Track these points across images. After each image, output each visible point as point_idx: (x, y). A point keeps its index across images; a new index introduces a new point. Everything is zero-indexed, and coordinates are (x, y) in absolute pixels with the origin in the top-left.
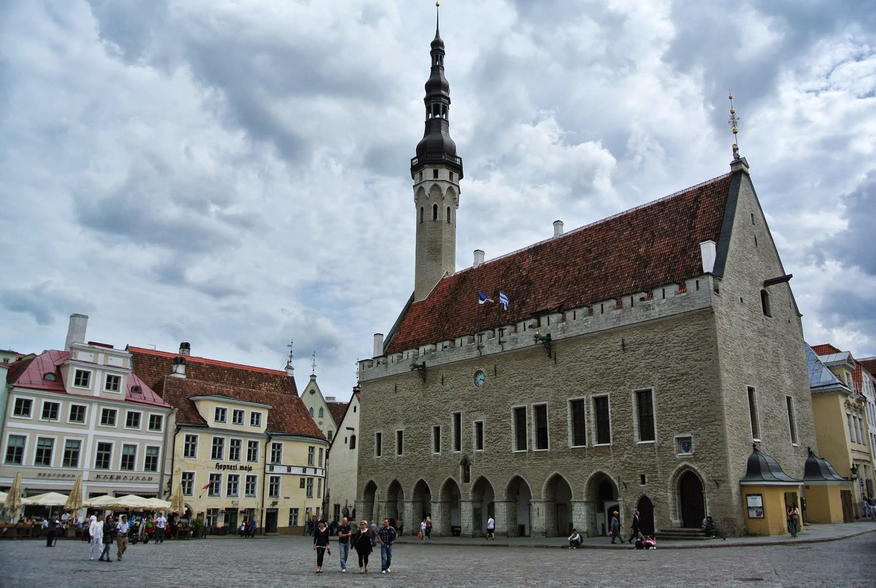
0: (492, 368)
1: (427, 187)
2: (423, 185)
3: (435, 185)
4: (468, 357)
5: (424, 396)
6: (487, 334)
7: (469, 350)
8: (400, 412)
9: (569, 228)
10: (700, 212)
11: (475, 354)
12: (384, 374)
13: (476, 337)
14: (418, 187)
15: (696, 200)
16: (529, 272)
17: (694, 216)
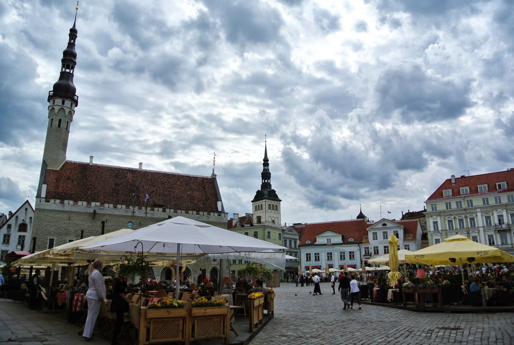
0: (139, 222)
1: (67, 111)
2: (64, 108)
3: (70, 111)
4: (125, 214)
5: (93, 226)
6: (136, 208)
7: (127, 212)
8: (73, 231)
9: (144, 168)
10: (206, 187)
11: (130, 214)
12: (60, 209)
13: (131, 207)
14: (61, 107)
15: (203, 181)
16: (133, 181)
17: (204, 187)
